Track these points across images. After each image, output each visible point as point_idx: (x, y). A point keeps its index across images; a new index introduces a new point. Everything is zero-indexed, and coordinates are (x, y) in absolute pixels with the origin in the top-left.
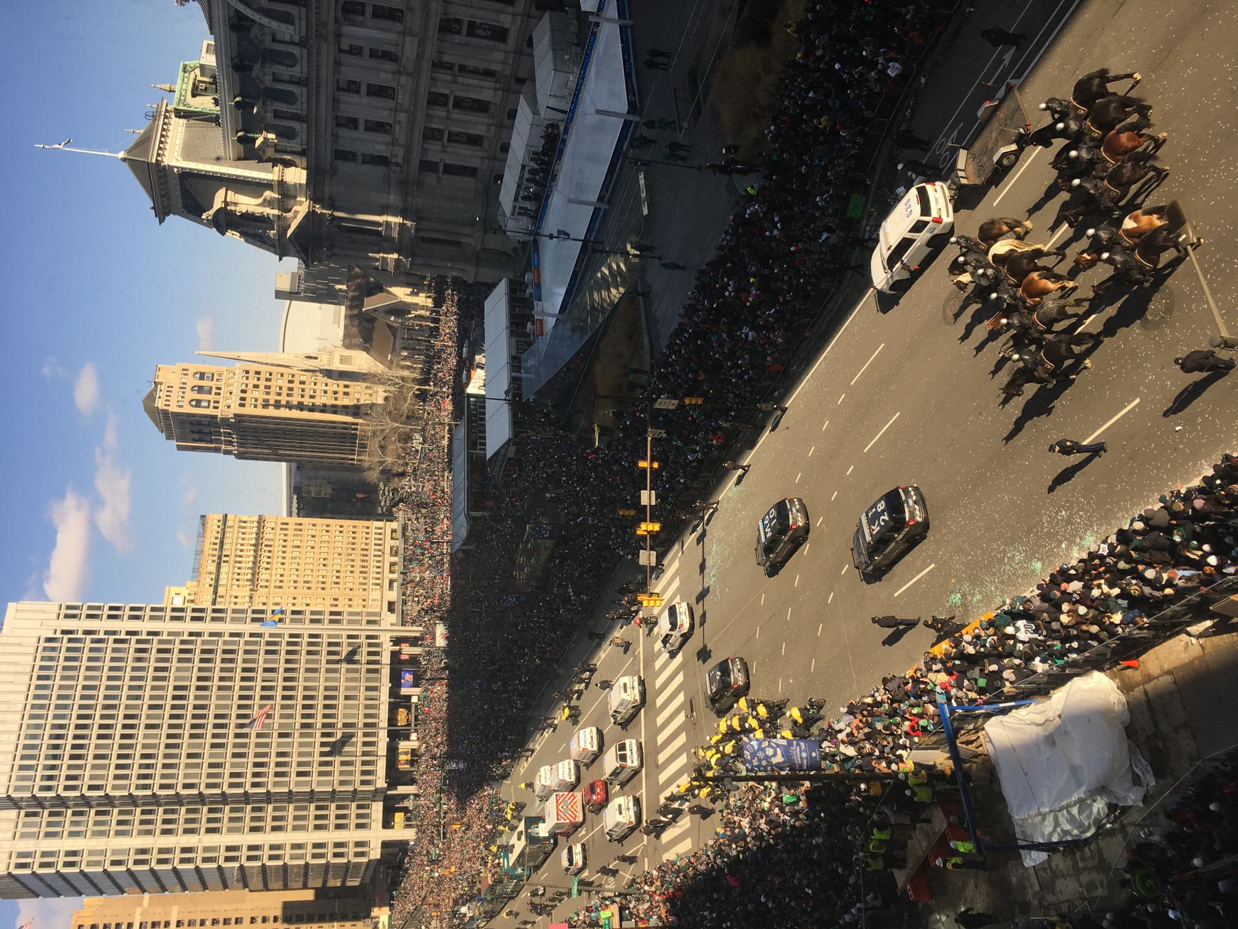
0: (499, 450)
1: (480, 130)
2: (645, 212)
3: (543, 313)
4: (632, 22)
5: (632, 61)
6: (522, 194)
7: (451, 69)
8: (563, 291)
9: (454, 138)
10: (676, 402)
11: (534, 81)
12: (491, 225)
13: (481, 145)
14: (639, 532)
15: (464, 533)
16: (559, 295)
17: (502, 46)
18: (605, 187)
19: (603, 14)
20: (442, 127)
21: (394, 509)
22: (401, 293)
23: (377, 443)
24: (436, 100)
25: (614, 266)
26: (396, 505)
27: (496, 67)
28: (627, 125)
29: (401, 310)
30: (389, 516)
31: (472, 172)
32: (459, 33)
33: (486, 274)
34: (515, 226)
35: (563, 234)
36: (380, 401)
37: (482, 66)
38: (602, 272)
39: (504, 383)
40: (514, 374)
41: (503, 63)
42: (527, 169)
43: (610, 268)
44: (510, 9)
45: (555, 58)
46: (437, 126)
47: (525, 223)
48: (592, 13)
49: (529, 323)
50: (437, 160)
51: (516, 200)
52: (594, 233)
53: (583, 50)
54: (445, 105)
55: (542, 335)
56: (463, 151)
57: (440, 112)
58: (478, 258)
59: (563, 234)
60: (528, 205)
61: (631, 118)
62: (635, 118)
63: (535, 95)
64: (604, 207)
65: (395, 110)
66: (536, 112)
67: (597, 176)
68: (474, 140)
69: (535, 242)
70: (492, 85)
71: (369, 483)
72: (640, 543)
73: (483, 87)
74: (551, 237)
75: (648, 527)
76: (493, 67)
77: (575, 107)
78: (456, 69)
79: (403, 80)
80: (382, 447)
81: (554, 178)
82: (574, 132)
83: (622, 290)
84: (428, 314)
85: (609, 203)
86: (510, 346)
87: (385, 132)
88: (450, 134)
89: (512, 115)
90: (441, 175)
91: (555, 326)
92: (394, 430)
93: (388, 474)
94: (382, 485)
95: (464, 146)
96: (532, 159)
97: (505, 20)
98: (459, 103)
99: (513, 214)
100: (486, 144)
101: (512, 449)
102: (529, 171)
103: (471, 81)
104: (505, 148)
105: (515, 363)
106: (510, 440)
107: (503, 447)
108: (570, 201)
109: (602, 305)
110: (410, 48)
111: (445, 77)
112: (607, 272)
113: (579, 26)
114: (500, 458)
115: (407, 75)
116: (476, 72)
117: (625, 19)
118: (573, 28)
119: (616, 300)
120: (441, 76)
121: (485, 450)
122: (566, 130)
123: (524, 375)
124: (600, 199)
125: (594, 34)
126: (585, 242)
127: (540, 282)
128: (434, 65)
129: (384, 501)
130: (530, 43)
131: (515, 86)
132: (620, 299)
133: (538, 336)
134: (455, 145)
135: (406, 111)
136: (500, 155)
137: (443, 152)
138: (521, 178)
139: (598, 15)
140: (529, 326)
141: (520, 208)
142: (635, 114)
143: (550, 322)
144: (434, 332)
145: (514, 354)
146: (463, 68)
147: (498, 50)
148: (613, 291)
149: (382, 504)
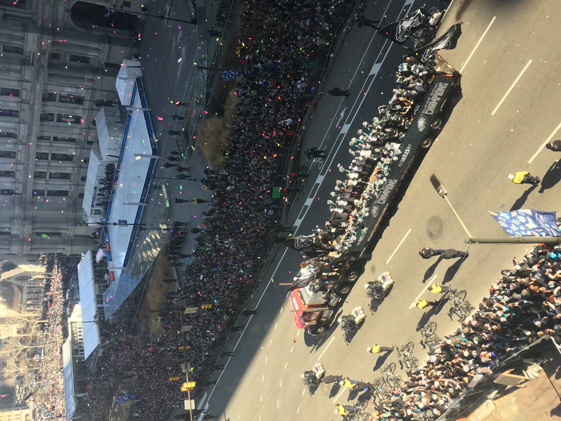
0: (93, 353)
1: (68, 171)
2: (168, 205)
3: (113, 268)
4: (150, 109)
5: (152, 128)
6: (96, 202)
7: (49, 139)
8: (124, 254)
9: (52, 176)
10: (197, 308)
11: (98, 142)
12: (79, 222)
13: (69, 178)
14: (183, 389)
15: (73, 409)
16: (123, 256)
17: (78, 126)
18: (143, 194)
19: (134, 106)
20: (45, 171)
21: (27, 401)
22: (25, 268)
23: (13, 361)
24: (41, 156)
25: (153, 237)
26: (27, 398)
27: (76, 137)
28: (152, 161)
29: (24, 278)
30: (24, 406)
31: (64, 193)
32: (52, 120)
33: (76, 249)
34: (92, 221)
35: (123, 223)
36: (14, 334)
37: (67, 136)
38: (147, 242)
39: (93, 311)
40: (99, 305)
41: (80, 134)
42: (98, 189)
43: (151, 238)
44: (81, 107)
45: (109, 129)
46: (42, 171)
47: (98, 219)
48: (128, 106)
49: (106, 274)
50: (43, 189)
51: (92, 206)
52: (140, 220)
53: (124, 124)
54: (47, 159)
55: (114, 280)
56: (58, 183)
57: (43, 163)
58: (73, 241)
59: (123, 223)
60: (99, 208)
61: (155, 157)
62: (157, 157)
63: (99, 149)
64: (144, 205)
65: (16, 164)
66: (100, 158)
67: (138, 190)
68: (65, 176)
69: (106, 229)
70: (74, 146)
71: (9, 387)
72: (184, 395)
73: (68, 148)
74: (115, 224)
75: (188, 386)
76: (74, 137)
77: (123, 154)
78: (52, 139)
79: (20, 147)
80: (17, 363)
81: (114, 192)
82: (123, 167)
83: (159, 249)
84: (43, 277)
85: (147, 202)
86: (95, 289)
87: (9, 176)
88: (50, 174)
89: (87, 161)
90: (46, 197)
91: (121, 275)
92: (24, 350)
93: (20, 379)
94: (17, 387)
95: (59, 180)
96: (100, 183)
97: (79, 112)
98: (55, 157)
99: (91, 214)
100: (72, 177)
101: (101, 351)
102: (99, 190)
103: (61, 145)
104: (84, 179)
105: (99, 299)
106: (99, 345)
107: (95, 350)
108: (124, 204)
109: (148, 259)
110: (23, 130)
111: (44, 143)
112: (149, 240)
113: (121, 113)
114: (93, 357)
115: (23, 144)
116: (64, 140)
117: (146, 107)
118: (118, 114)
119: (156, 255)
120: (43, 144)
121: (83, 354)
122: (119, 166)
123: (105, 305)
124: (142, 201)
125: (130, 116)
126: (135, 225)
127: (110, 250)
128: (38, 138)
129: (19, 397)
130: (94, 123)
131: (87, 146)
132: (158, 254)
133: (112, 281)
134: (53, 180)
135: (23, 164)
136: (81, 183)
137: (47, 184)
138: (95, 194)
139: (131, 107)
140: (106, 276)
141: (95, 210)
142: (156, 155)
143: (118, 273)
144: (48, 287)
145: (98, 293)
146: (56, 139)
147: (76, 128)
148: (154, 250)
149: (18, 399)
